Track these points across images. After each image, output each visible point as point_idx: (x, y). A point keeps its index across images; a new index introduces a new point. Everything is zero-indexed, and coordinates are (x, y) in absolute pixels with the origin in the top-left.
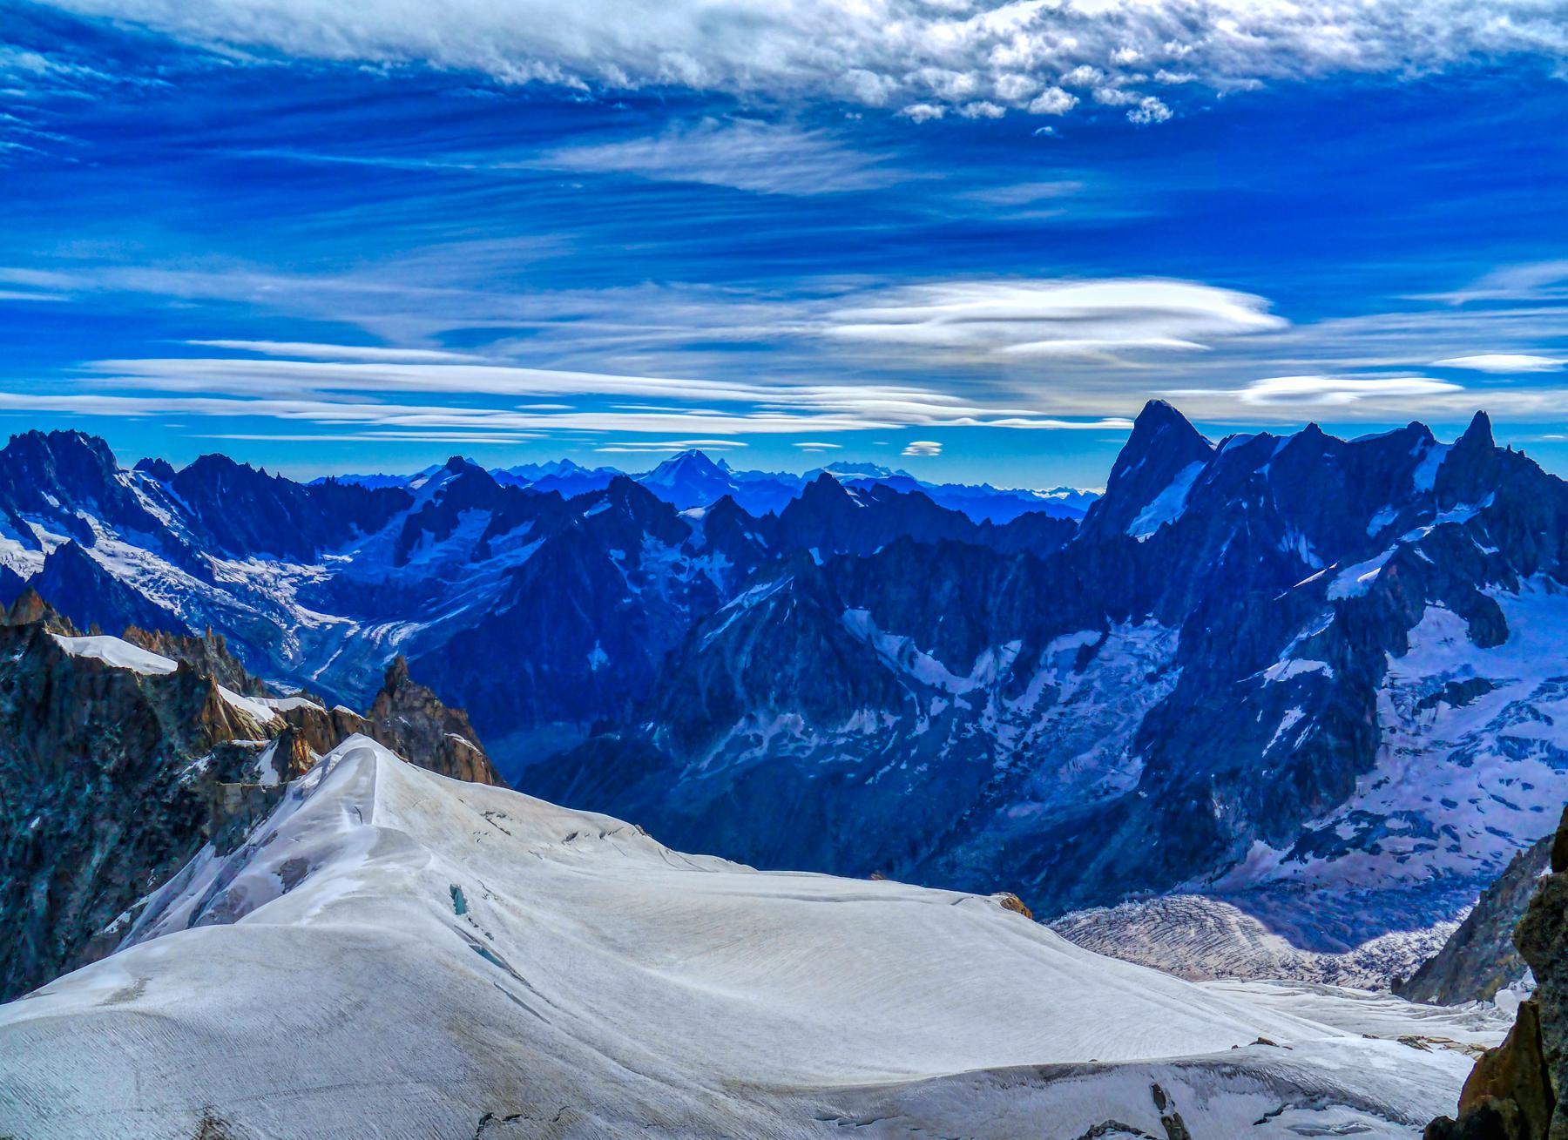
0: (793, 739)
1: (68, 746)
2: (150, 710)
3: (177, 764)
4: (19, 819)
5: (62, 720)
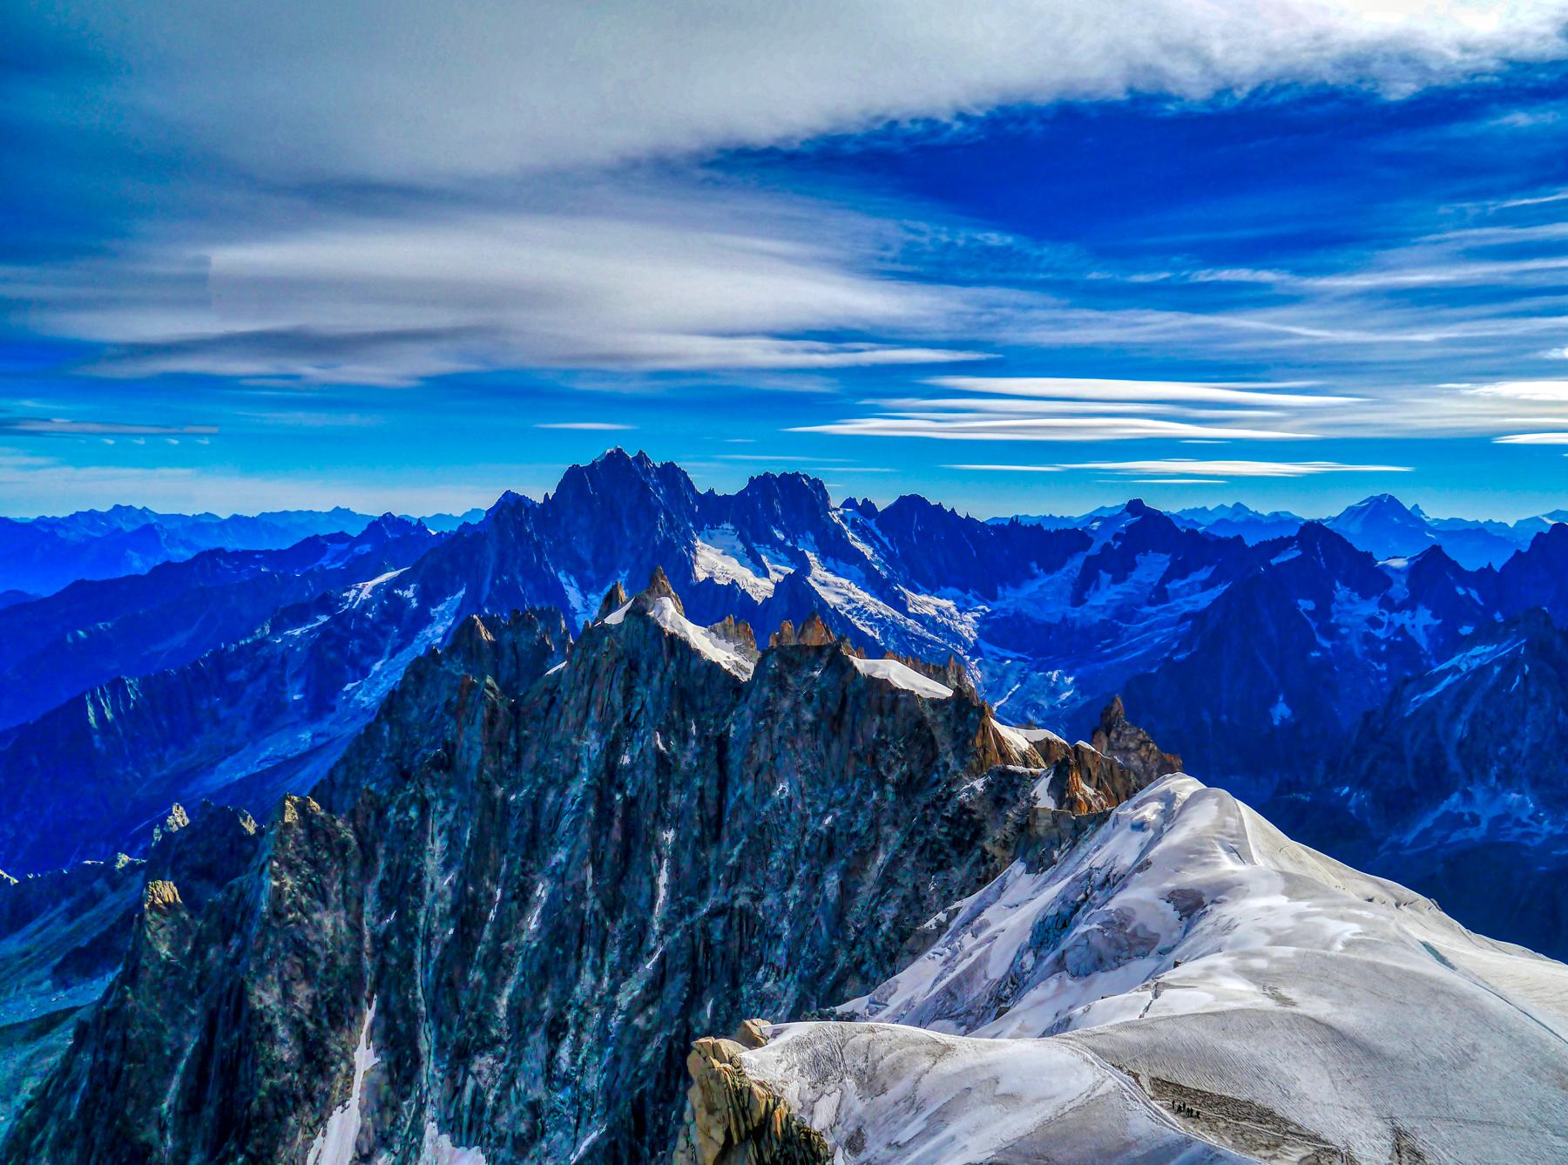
0: (1518, 823)
1: (857, 754)
2: (929, 730)
3: (955, 782)
4: (815, 814)
5: (853, 732)
